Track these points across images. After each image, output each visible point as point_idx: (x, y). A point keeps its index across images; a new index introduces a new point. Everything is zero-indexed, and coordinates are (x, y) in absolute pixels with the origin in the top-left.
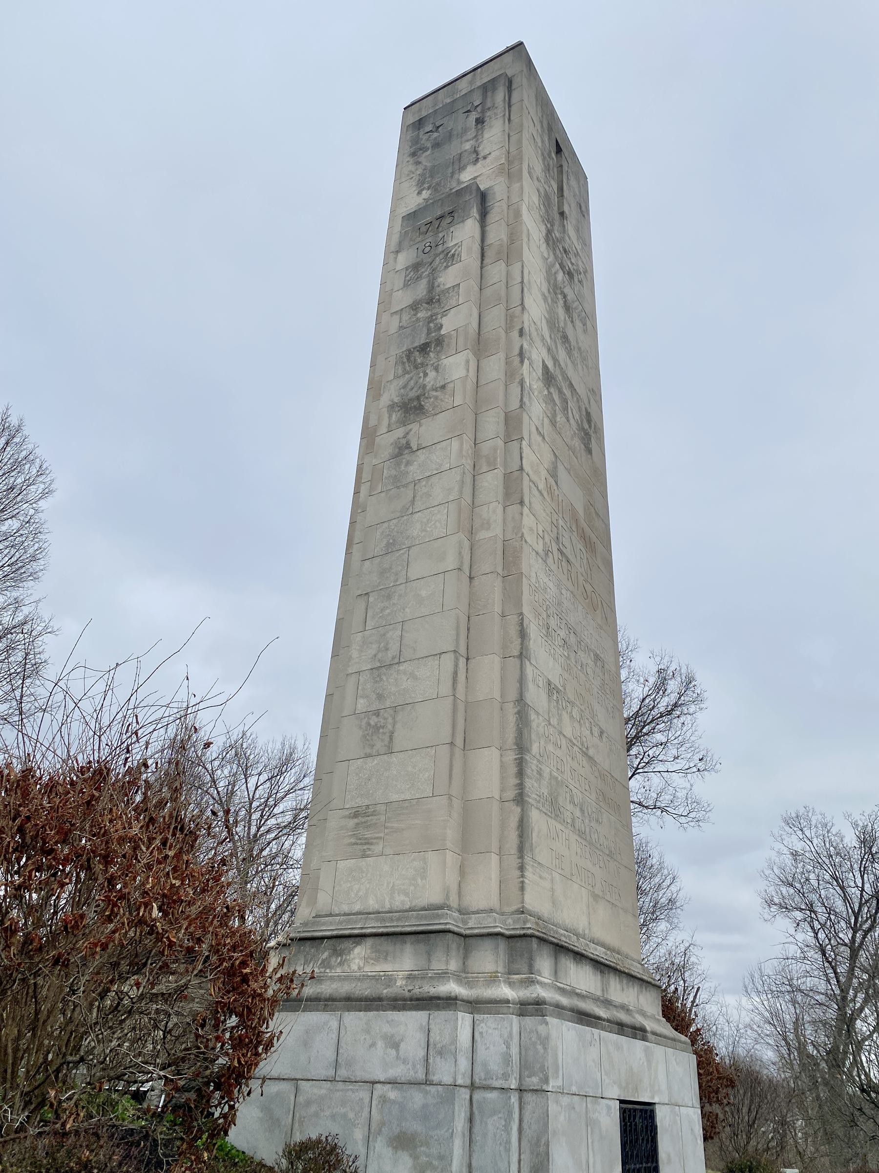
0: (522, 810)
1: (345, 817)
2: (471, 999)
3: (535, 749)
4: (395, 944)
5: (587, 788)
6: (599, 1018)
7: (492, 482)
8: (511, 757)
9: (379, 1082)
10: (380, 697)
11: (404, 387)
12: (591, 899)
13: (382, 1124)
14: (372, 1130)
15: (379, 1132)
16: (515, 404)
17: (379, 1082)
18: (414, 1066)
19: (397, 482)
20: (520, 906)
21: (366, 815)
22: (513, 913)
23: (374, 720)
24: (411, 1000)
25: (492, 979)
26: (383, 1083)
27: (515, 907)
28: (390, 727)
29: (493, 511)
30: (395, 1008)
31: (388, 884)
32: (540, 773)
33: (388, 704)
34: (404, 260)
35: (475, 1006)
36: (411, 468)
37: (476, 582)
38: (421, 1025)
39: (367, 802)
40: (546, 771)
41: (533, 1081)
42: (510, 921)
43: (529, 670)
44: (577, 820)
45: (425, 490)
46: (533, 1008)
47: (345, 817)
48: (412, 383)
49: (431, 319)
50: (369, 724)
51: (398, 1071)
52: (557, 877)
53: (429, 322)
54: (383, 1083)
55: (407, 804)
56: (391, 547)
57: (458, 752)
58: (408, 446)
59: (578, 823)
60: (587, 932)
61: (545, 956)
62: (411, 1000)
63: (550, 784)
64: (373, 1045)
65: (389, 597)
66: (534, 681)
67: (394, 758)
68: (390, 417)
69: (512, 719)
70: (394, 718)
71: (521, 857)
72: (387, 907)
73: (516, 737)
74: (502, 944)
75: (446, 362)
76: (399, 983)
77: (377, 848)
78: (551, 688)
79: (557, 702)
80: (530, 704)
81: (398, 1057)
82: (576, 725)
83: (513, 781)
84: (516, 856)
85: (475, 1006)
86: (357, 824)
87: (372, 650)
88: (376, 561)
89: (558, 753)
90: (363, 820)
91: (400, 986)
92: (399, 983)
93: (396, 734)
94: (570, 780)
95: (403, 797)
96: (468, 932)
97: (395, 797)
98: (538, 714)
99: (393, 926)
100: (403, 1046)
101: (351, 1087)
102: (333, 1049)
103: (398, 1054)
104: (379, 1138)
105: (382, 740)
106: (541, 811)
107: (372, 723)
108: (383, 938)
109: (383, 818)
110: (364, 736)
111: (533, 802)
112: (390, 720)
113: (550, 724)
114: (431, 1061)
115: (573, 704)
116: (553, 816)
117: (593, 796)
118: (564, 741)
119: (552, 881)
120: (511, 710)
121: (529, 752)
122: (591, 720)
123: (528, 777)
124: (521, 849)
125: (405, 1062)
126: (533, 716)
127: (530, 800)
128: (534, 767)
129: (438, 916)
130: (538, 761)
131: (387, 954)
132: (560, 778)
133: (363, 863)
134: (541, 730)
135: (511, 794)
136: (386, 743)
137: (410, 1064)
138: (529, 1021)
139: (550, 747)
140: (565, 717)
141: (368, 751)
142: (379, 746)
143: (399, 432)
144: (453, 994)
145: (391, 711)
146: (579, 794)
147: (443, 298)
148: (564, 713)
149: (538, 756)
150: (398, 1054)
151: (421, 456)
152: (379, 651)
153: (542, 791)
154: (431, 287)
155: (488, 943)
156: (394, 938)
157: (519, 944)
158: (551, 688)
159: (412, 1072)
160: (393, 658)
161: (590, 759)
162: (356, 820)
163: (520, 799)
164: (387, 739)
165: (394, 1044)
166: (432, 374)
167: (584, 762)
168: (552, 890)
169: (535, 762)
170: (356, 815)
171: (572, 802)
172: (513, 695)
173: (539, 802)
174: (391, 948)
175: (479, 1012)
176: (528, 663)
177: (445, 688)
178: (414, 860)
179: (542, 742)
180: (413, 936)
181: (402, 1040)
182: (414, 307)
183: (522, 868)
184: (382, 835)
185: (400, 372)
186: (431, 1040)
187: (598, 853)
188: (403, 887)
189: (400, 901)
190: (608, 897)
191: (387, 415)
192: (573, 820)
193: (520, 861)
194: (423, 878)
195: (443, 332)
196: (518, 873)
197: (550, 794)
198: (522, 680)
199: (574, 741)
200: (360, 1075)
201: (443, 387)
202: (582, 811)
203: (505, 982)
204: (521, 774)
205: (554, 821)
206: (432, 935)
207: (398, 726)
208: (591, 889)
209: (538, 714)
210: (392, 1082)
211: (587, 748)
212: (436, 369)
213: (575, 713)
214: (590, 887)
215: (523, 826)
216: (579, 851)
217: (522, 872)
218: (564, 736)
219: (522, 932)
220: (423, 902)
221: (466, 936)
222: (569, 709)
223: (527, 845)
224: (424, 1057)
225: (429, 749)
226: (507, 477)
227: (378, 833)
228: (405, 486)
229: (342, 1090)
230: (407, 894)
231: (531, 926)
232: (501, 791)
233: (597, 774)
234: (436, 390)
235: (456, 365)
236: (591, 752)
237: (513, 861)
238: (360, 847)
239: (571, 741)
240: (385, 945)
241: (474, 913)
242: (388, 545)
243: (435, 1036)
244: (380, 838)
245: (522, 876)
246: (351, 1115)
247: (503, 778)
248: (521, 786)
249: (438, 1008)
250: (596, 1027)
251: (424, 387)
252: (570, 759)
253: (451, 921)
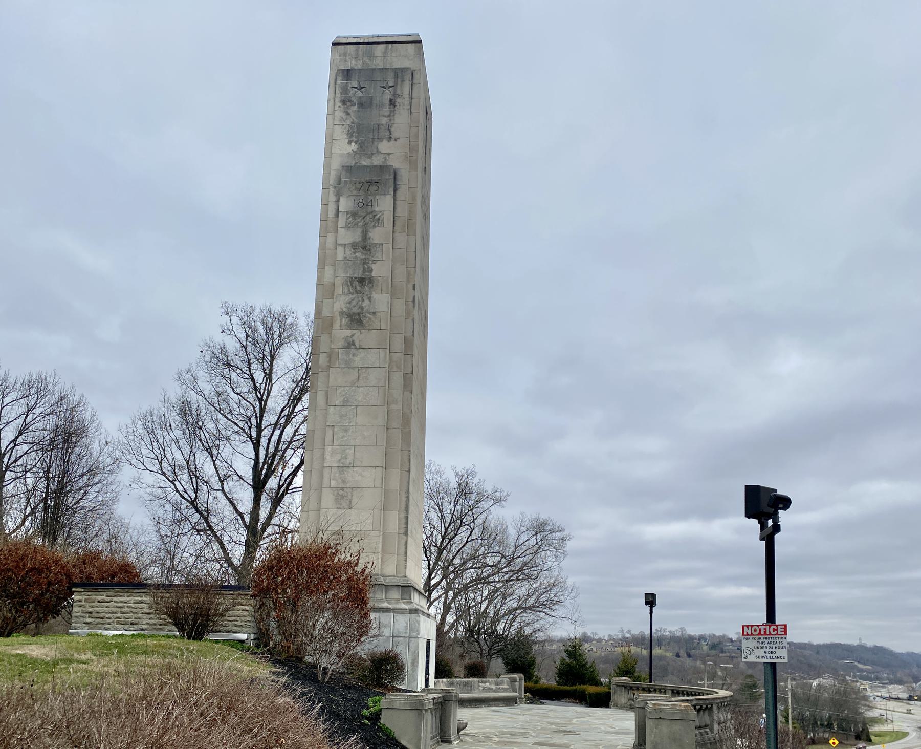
7: (398, 378)
8: (403, 515)
10: (344, 482)
11: (350, 303)
16: (410, 334)
19: (348, 363)
23: (341, 492)
25: (397, 601)
29: (398, 394)
33: (348, 485)
34: (345, 204)
35: (395, 611)
36: (356, 359)
37: (390, 431)
41: (414, 634)
45: (365, 375)
46: (415, 611)
48: (354, 303)
49: (365, 262)
53: (364, 263)
56: (345, 403)
58: (353, 344)
65: (346, 431)
67: (352, 512)
68: (341, 320)
69: (404, 499)
75: (375, 296)
85: (395, 611)
87: (338, 457)
88: (338, 408)
138: (413, 616)
143: (348, 333)
147: (372, 250)
151: (362, 353)
152: (342, 458)
154: (365, 236)
163: (406, 533)
166: (367, 302)
172: (405, 489)
177: (378, 483)
182: (354, 246)
185: (346, 291)
191: (339, 318)
195: (373, 274)
201: (374, 313)
204: (407, 523)
212: (370, 299)
226: (405, 374)
228: (353, 368)
234: (369, 313)
235: (380, 301)
242: (344, 401)
251: (362, 308)
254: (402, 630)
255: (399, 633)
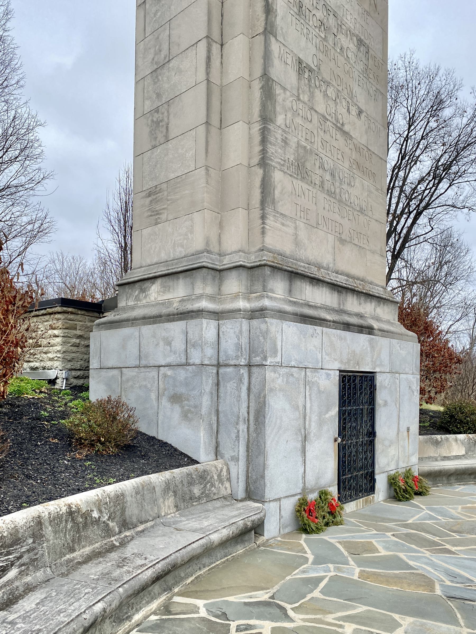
0: (264, 171)
1: (143, 198)
2: (217, 311)
3: (280, 120)
4: (173, 281)
5: (340, 157)
6: (325, 320)
8: (256, 128)
9: (162, 366)
12: (337, 243)
13: (165, 390)
14: (160, 394)
15: (164, 395)
17: (162, 366)
18: (180, 355)
20: (261, 246)
21: (156, 193)
22: (256, 252)
24: (178, 314)
25: (236, 297)
26: (164, 366)
27: (259, 246)
28: (166, 119)
30: (169, 321)
31: (172, 240)
32: (285, 141)
33: (164, 100)
35: (218, 315)
38: (182, 329)
39: (155, 183)
40: (293, 141)
42: (253, 257)
43: (275, 47)
44: (326, 183)
47: (143, 198)
50: (152, 121)
51: (171, 359)
52: (302, 225)
54: (164, 366)
55: (179, 179)
57: (214, 131)
59: (327, 185)
60: (331, 265)
61: (279, 280)
62: (178, 314)
63: (298, 151)
64: (157, 345)
66: (280, 58)
67: (170, 145)
69: (257, 94)
70: (168, 112)
71: (263, 209)
72: (172, 256)
73: (260, 110)
74: (244, 274)
76: (175, 305)
77: (164, 217)
78: (301, 68)
79: (309, 80)
80: (275, 79)
81: (171, 351)
82: (332, 104)
83: (258, 148)
84: (259, 209)
85: (218, 315)
86: (151, 201)
89: (309, 126)
90: (154, 197)
91: (176, 306)
92: (175, 305)
93: (170, 125)
94: (320, 150)
95: (177, 175)
96: (222, 267)
97: (172, 176)
98: (285, 89)
99: (172, 269)
100: (173, 343)
101: (148, 370)
102: (137, 348)
103: (171, 348)
104: (164, 398)
105: (162, 132)
106: (285, 173)
107: (155, 119)
108: (166, 277)
109: (166, 193)
110: (151, 132)
111: (277, 165)
112: (166, 114)
113: (299, 99)
114: (188, 351)
115: (328, 84)
116: (299, 177)
117: (347, 164)
118: (315, 117)
119: (296, 228)
120: (257, 85)
121: (273, 123)
122: (348, 99)
123: (271, 143)
124: (263, 203)
125: (175, 353)
126: (278, 91)
127: (273, 164)
128: (279, 137)
129: (199, 258)
130: (284, 131)
131: (169, 288)
132: (308, 147)
133: (156, 228)
134: (288, 104)
135: (256, 160)
136: (164, 133)
137: (178, 354)
139: (299, 120)
140: (319, 95)
141: (153, 143)
142: (161, 138)
144: (201, 308)
145: (165, 106)
146: (330, 161)
148: (317, 92)
149: (283, 127)
150: (171, 348)
153: (287, 157)
155: (234, 273)
156: (172, 276)
157: (256, 273)
158: (301, 68)
159: (179, 359)
160: (165, 58)
161: (345, 134)
162: (150, 199)
163: (264, 162)
164: (165, 131)
165: (168, 343)
167: (339, 136)
168: (296, 235)
169: (280, 131)
170: (149, 195)
171: (322, 167)
172: (258, 72)
173: (283, 165)
174: (171, 284)
175: (223, 318)
176: (273, 39)
178: (185, 221)
179: (289, 115)
180: (183, 274)
181: (173, 340)
183: (263, 217)
184: (165, 206)
186: (188, 339)
187: (348, 208)
188: (180, 242)
189: (180, 252)
190: (356, 242)
192: (322, 182)
193: (262, 212)
194: (192, 232)
196: (260, 221)
197: (297, 160)
198: (267, 56)
199: (327, 117)
200: (152, 363)
202: (332, 175)
203: (242, 298)
205: (299, 182)
206: (194, 271)
207: (171, 116)
208: (338, 235)
209: (285, 89)
210: (168, 366)
211: (343, 124)
213: (331, 92)
214: (337, 234)
215: (266, 187)
216: (327, 207)
217: (263, 220)
218: (316, 111)
219: (258, 263)
220: (191, 250)
221: (220, 271)
222: (323, 88)
223: (269, 199)
224: (184, 349)
225: (191, 132)
227: (163, 205)
229: (144, 372)
230: (182, 246)
231: (267, 258)
232: (250, 159)
233: (351, 146)
236: (346, 128)
237: (257, 213)
238: (154, 217)
239: (324, 116)
240: (169, 282)
241: (228, 254)
243: (190, 336)
244: (164, 209)
245: (263, 223)
246: (149, 386)
247: (250, 147)
248: (264, 151)
249: (192, 318)
250: (320, 325)
252: (321, 133)
253: (205, 261)
254: (231, 352)
255: (228, 358)
